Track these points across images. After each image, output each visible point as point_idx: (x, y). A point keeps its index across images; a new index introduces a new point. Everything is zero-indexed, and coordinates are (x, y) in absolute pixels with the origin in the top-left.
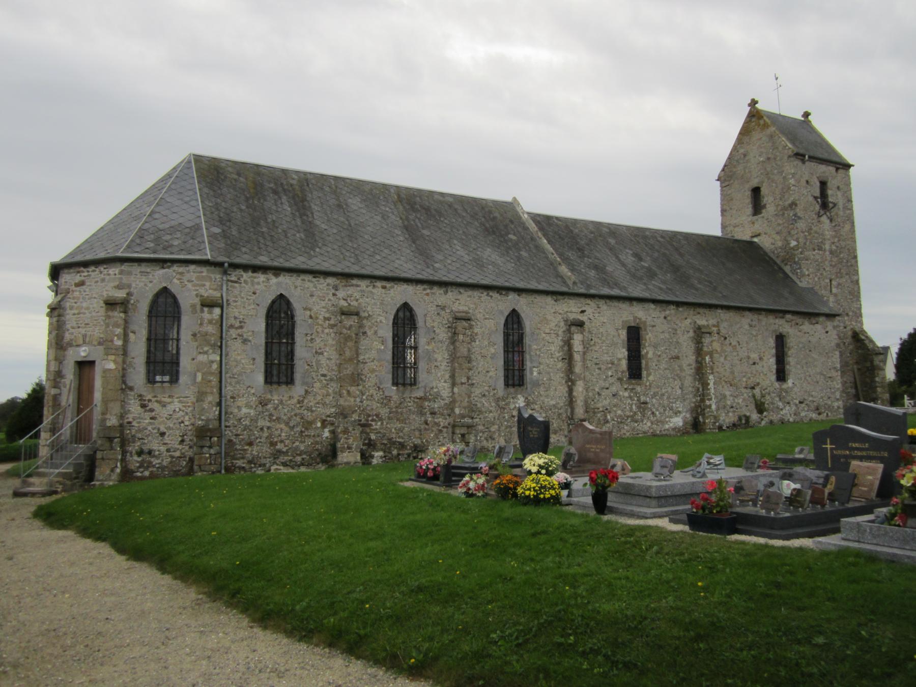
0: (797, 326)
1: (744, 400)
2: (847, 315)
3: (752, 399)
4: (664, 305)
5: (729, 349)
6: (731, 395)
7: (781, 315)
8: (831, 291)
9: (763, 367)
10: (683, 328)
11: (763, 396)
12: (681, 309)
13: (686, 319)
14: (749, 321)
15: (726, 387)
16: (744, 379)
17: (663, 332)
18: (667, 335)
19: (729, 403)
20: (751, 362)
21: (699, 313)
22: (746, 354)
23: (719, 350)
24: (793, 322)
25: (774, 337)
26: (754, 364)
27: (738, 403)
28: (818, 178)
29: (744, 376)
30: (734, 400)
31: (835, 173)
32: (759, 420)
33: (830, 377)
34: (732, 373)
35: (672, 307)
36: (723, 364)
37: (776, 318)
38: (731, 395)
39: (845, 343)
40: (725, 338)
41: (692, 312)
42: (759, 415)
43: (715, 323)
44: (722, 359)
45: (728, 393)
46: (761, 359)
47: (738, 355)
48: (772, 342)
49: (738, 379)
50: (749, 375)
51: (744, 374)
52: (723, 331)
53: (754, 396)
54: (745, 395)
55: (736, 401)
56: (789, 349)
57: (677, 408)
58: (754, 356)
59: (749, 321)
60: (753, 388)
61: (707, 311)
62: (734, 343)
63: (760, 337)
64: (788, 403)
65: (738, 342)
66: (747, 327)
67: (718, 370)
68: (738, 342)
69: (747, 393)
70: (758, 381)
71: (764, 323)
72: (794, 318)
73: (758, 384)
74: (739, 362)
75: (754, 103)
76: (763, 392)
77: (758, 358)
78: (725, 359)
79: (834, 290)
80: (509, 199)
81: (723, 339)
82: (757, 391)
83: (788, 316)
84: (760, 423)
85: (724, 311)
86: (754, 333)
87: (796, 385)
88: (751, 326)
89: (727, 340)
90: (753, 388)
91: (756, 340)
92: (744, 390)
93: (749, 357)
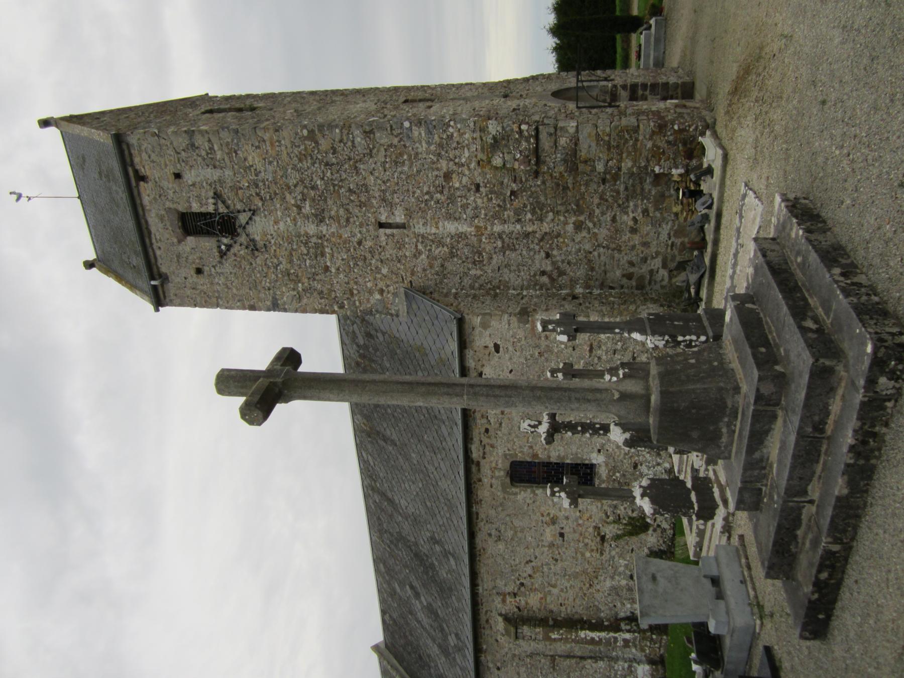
0: (491, 432)
1: (621, 556)
2: (447, 176)
3: (622, 542)
4: (481, 668)
5: (538, 581)
6: (612, 578)
7: (474, 468)
8: (402, 226)
9: (567, 518)
10: (511, 645)
11: (618, 520)
12: (485, 647)
13: (497, 641)
14: (491, 541)
15: (598, 587)
16: (588, 554)
17: (518, 674)
18: (523, 669)
19: (624, 582)
20: (559, 541)
21: (487, 621)
22: (546, 549)
23: (540, 595)
24: (486, 441)
25: (514, 490)
26: (562, 535)
27: (626, 566)
28: (180, 242)
29: (583, 555)
30: (620, 574)
31: (151, 184)
32: (659, 531)
33: (591, 350)
34: (576, 576)
35: (483, 658)
36: (562, 590)
37: (480, 480)
38: (612, 578)
39: (513, 193)
40: (522, 584)
41: (487, 632)
42: (650, 532)
43: (499, 599)
44: (555, 591)
45: (608, 583)
46: (554, 521)
47: (547, 564)
48: (523, 495)
49: (587, 566)
50: (581, 545)
51: (579, 556)
52: (510, 588)
53: (617, 537)
54: (613, 553)
55: (621, 569)
56: (535, 455)
57: (623, 669)
58: (549, 534)
59: (491, 541)
60: (603, 538)
61: (483, 609)
62: (529, 570)
63: (517, 523)
64: (635, 466)
65: (527, 562)
66: (501, 546)
67: (571, 599)
68: (527, 562)
69: (612, 550)
70: (591, 530)
71: (492, 512)
72: (476, 440)
73: (596, 528)
74: (560, 564)
75: (89, 265)
76: (611, 518)
77: (552, 527)
78: (554, 586)
79: (399, 217)
80: (375, 657)
81: (522, 589)
82: (610, 531)
83: (475, 449)
84: (664, 530)
85: (479, 581)
86: (510, 533)
87: (603, 445)
88: (499, 539)
89: (524, 582)
90: (603, 538)
91: (522, 531)
92: (606, 556)
93: (551, 545)
